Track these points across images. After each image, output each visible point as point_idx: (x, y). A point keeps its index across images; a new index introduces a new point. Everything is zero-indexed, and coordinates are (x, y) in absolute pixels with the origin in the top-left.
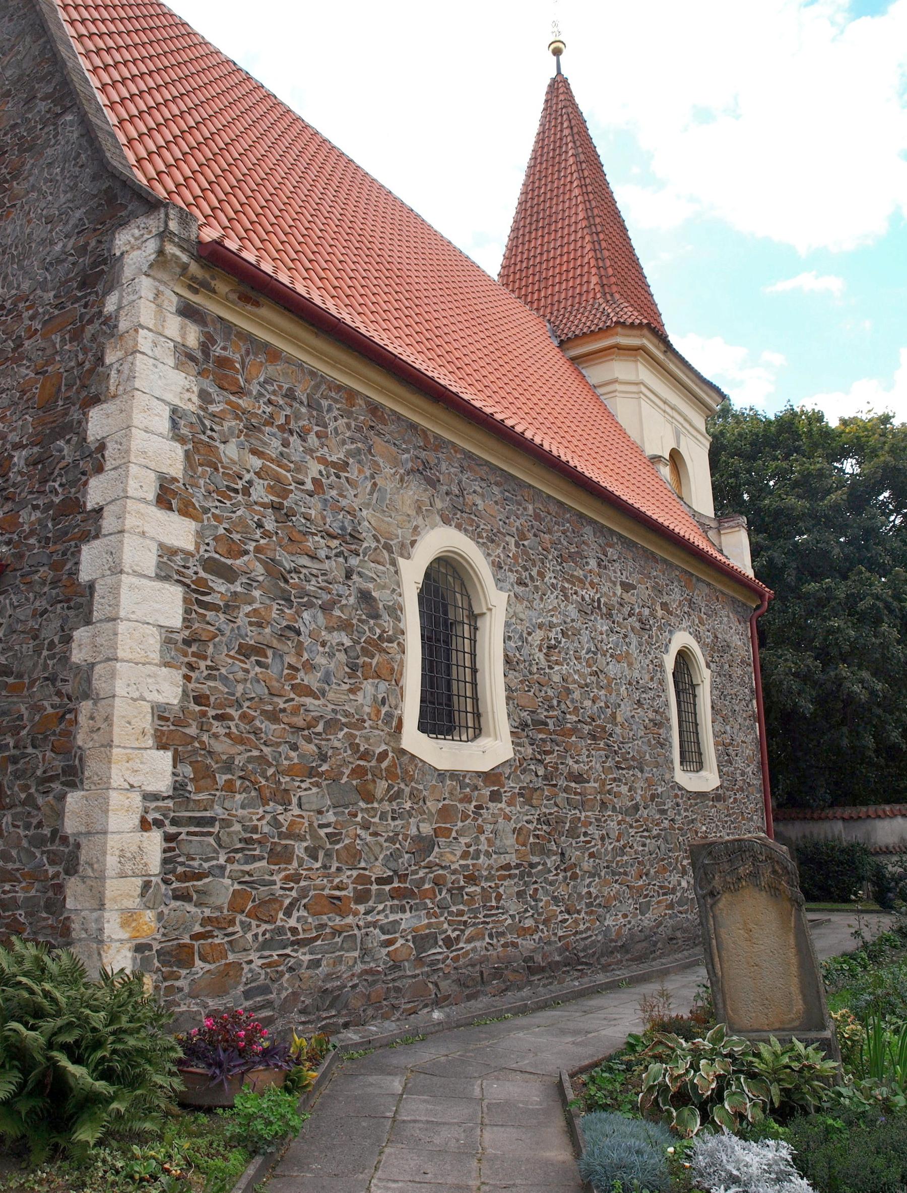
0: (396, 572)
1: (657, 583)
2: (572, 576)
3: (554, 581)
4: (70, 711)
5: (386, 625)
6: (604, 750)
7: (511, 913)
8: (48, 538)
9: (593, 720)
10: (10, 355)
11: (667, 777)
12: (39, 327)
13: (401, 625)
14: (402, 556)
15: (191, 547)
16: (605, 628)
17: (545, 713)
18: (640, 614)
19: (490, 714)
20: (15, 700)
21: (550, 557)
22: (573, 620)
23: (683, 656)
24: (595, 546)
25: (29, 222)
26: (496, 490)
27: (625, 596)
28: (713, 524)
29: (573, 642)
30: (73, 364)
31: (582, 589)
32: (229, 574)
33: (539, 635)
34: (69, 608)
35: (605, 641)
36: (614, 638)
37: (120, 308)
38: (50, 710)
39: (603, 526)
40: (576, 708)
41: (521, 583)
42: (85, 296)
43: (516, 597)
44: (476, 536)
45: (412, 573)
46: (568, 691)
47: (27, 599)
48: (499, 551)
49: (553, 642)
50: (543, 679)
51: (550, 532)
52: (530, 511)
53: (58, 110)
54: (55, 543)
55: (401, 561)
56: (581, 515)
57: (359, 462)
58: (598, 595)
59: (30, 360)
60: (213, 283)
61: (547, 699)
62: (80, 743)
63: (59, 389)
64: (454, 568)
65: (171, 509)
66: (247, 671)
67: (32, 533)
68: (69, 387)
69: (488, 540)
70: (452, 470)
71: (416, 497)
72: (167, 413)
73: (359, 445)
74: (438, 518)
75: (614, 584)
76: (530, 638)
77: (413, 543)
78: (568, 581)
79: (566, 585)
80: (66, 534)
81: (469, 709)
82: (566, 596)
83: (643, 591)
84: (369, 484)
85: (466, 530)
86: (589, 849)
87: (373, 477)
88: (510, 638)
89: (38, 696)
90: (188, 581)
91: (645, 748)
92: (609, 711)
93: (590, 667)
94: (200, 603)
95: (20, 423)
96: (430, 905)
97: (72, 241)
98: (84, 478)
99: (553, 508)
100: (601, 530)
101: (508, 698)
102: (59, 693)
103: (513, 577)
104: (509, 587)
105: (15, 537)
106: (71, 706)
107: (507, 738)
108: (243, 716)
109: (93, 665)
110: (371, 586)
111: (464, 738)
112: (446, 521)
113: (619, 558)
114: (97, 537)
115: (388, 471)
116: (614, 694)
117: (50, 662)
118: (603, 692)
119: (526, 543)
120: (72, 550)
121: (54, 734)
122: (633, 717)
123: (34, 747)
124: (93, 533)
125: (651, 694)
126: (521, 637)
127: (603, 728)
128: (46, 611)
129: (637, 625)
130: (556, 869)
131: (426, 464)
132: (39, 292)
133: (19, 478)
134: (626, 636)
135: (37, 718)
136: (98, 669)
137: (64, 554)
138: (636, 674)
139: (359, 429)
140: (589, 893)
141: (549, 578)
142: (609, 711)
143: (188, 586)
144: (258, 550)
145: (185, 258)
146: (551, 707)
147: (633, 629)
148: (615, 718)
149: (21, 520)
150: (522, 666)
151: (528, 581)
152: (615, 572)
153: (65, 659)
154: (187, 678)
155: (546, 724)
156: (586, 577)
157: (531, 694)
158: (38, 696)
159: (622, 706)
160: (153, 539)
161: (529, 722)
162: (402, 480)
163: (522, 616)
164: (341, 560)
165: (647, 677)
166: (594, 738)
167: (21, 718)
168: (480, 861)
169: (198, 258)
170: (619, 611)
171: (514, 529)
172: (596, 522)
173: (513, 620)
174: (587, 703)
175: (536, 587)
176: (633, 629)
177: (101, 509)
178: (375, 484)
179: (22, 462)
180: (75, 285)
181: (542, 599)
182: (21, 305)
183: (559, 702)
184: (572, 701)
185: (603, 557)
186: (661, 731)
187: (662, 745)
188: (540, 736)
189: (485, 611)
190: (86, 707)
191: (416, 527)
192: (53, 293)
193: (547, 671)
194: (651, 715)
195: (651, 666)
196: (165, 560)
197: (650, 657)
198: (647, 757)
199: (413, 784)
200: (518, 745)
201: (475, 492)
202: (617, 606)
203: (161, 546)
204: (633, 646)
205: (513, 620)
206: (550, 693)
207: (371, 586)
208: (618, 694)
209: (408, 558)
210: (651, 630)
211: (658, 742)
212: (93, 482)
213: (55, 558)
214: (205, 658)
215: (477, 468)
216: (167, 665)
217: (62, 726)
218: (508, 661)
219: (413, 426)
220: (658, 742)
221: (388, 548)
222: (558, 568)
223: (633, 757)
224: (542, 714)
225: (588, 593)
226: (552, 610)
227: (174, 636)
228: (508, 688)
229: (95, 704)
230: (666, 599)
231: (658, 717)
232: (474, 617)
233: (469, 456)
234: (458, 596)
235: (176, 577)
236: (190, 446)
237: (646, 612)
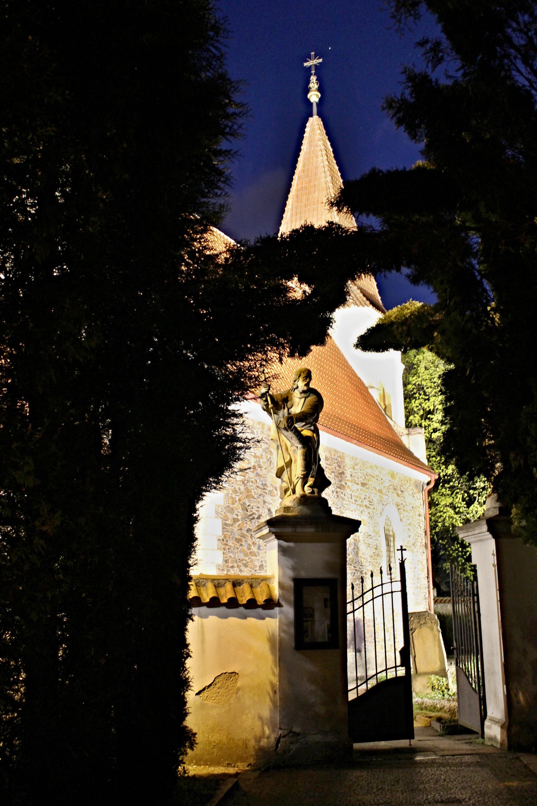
28: (406, 431)
32: (232, 511)
66: (238, 549)
79: (338, 490)
94: (226, 524)
108: (238, 566)
144: (240, 500)
154: (224, 553)
164: (262, 497)
214: (227, 545)
216: (219, 549)
227: (220, 538)
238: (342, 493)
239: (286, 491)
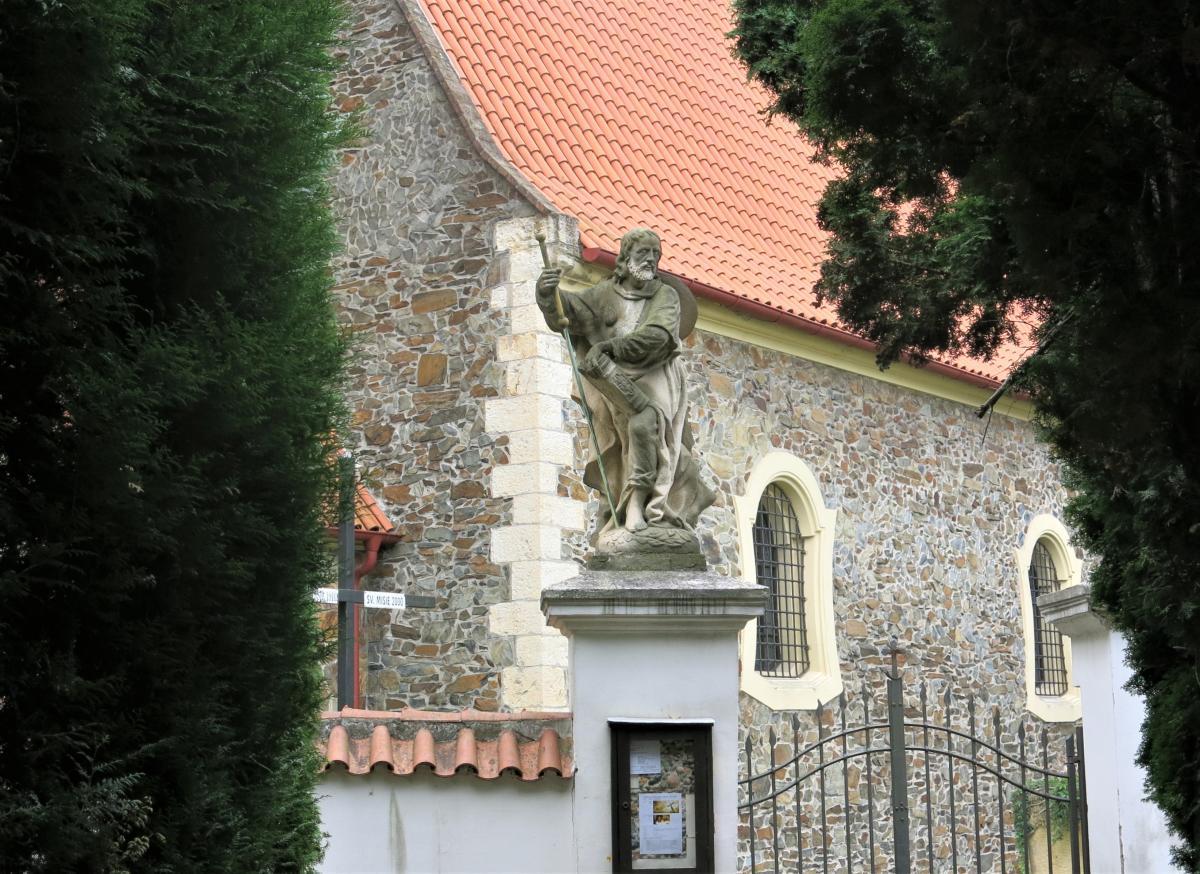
0: (733, 512)
1: (1011, 456)
2: (906, 472)
3: (885, 483)
4: (492, 675)
5: (725, 567)
6: (940, 676)
7: (841, 857)
8: (450, 517)
9: (928, 642)
10: (374, 321)
11: (1017, 705)
12: (409, 300)
13: (739, 566)
14: (738, 493)
15: (581, 527)
16: (944, 528)
17: (875, 640)
18: (988, 501)
19: (820, 647)
20: (427, 661)
21: (881, 455)
22: (906, 527)
23: (1044, 546)
24: (933, 428)
25: (378, 176)
26: (823, 391)
27: (970, 483)
29: (905, 552)
30: (457, 348)
31: (917, 486)
33: (870, 549)
34: (482, 584)
35: (944, 545)
36: (954, 538)
37: (510, 307)
38: (469, 673)
39: (943, 400)
40: (909, 631)
41: (850, 494)
42: (465, 282)
43: (845, 512)
44: (804, 453)
45: (747, 509)
46: (900, 611)
47: (429, 570)
48: (827, 463)
49: (884, 557)
50: (873, 601)
51: (881, 424)
52: (860, 406)
53: (400, 55)
54: (457, 522)
55: (737, 499)
56: (916, 394)
57: (699, 403)
58: (936, 489)
59: (402, 332)
60: (589, 276)
61: (878, 623)
62: (507, 703)
63: (444, 372)
64: (781, 490)
65: (567, 495)
67: (427, 509)
68: (456, 371)
69: (813, 452)
70: (781, 383)
71: (749, 425)
72: (559, 408)
73: (699, 386)
74: (769, 443)
75: (955, 469)
76: (859, 556)
77: (747, 476)
78: (900, 479)
79: (899, 485)
80: (471, 515)
81: (798, 642)
82: (898, 499)
83: (993, 469)
84: (708, 424)
85: (795, 448)
86: (921, 792)
87: (710, 415)
88: (838, 560)
89: (454, 659)
90: (581, 558)
91: (990, 671)
92: (946, 630)
93: (925, 579)
95: (397, 395)
96: (768, 846)
97: (440, 216)
98: (485, 466)
99: (885, 394)
100: (941, 406)
101: (838, 627)
102: (478, 659)
103: (841, 489)
104: (838, 501)
105: (406, 508)
106: (492, 670)
107: (838, 672)
109: (515, 638)
110: (712, 530)
111: (793, 674)
112: (776, 442)
113: (963, 435)
114: (508, 523)
115: (723, 403)
116: (953, 606)
117: (465, 631)
118: (940, 607)
119: (854, 445)
120: (480, 531)
121: (477, 693)
122: (975, 633)
123: (453, 703)
124: (503, 520)
125: (1001, 601)
126: (850, 557)
127: (939, 651)
128: (454, 584)
129: (984, 516)
130: (886, 813)
131: (756, 385)
132: (403, 262)
133: (404, 452)
134: (969, 533)
135: (454, 678)
136: (518, 640)
137: (471, 533)
138: (981, 579)
139: (698, 368)
140: (921, 842)
141: (880, 483)
142: (946, 630)
143: (581, 562)
145: (570, 262)
146: (882, 632)
147: (978, 522)
148: (953, 637)
149: (411, 493)
150: (851, 590)
151: (857, 491)
152: (957, 454)
153: (481, 630)
155: (875, 652)
156: (921, 469)
157: (860, 620)
158: (454, 659)
159: (963, 621)
160: (558, 526)
161: (859, 652)
162: (735, 410)
163: (851, 533)
165: (994, 581)
166: (928, 663)
167: (436, 677)
168: (811, 803)
169: (582, 261)
170: (961, 503)
171: (842, 432)
172: (935, 397)
173: (842, 539)
174: (922, 623)
175: (866, 495)
176: (978, 522)
177: (511, 499)
178: (712, 423)
179: (406, 437)
180: (451, 267)
181: (872, 508)
182: (381, 269)
183: (890, 626)
184: (905, 623)
185: (942, 439)
186: (1011, 648)
187: (1012, 666)
188: (871, 666)
189: (813, 534)
190: (509, 674)
191: (750, 459)
192: (423, 267)
193: (877, 591)
194: (999, 628)
195: (1000, 567)
196: (565, 542)
197: (999, 555)
198: (993, 679)
199: (752, 726)
200: (848, 678)
201: (802, 402)
202: (958, 497)
203: (563, 530)
204: (977, 545)
205: (842, 539)
206: (881, 616)
207: (712, 530)
208: (958, 607)
209: (742, 495)
210: (1001, 518)
211: (1008, 663)
212: (498, 471)
213: (459, 536)
215: (805, 373)
217: (486, 687)
218: (837, 586)
219: (744, 348)
220: (1008, 663)
221: (726, 488)
222: (890, 465)
223: (975, 685)
224: (872, 641)
225: (924, 489)
226: (883, 519)
228: (838, 617)
229: (520, 670)
230: (1022, 474)
231: (1008, 631)
232: (801, 539)
233: (799, 362)
234: (786, 520)
235: (574, 556)
236: (575, 434)
237: (996, 496)
238: (910, 492)
239: (608, 516)
